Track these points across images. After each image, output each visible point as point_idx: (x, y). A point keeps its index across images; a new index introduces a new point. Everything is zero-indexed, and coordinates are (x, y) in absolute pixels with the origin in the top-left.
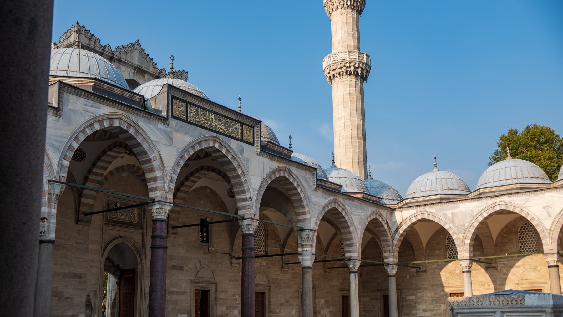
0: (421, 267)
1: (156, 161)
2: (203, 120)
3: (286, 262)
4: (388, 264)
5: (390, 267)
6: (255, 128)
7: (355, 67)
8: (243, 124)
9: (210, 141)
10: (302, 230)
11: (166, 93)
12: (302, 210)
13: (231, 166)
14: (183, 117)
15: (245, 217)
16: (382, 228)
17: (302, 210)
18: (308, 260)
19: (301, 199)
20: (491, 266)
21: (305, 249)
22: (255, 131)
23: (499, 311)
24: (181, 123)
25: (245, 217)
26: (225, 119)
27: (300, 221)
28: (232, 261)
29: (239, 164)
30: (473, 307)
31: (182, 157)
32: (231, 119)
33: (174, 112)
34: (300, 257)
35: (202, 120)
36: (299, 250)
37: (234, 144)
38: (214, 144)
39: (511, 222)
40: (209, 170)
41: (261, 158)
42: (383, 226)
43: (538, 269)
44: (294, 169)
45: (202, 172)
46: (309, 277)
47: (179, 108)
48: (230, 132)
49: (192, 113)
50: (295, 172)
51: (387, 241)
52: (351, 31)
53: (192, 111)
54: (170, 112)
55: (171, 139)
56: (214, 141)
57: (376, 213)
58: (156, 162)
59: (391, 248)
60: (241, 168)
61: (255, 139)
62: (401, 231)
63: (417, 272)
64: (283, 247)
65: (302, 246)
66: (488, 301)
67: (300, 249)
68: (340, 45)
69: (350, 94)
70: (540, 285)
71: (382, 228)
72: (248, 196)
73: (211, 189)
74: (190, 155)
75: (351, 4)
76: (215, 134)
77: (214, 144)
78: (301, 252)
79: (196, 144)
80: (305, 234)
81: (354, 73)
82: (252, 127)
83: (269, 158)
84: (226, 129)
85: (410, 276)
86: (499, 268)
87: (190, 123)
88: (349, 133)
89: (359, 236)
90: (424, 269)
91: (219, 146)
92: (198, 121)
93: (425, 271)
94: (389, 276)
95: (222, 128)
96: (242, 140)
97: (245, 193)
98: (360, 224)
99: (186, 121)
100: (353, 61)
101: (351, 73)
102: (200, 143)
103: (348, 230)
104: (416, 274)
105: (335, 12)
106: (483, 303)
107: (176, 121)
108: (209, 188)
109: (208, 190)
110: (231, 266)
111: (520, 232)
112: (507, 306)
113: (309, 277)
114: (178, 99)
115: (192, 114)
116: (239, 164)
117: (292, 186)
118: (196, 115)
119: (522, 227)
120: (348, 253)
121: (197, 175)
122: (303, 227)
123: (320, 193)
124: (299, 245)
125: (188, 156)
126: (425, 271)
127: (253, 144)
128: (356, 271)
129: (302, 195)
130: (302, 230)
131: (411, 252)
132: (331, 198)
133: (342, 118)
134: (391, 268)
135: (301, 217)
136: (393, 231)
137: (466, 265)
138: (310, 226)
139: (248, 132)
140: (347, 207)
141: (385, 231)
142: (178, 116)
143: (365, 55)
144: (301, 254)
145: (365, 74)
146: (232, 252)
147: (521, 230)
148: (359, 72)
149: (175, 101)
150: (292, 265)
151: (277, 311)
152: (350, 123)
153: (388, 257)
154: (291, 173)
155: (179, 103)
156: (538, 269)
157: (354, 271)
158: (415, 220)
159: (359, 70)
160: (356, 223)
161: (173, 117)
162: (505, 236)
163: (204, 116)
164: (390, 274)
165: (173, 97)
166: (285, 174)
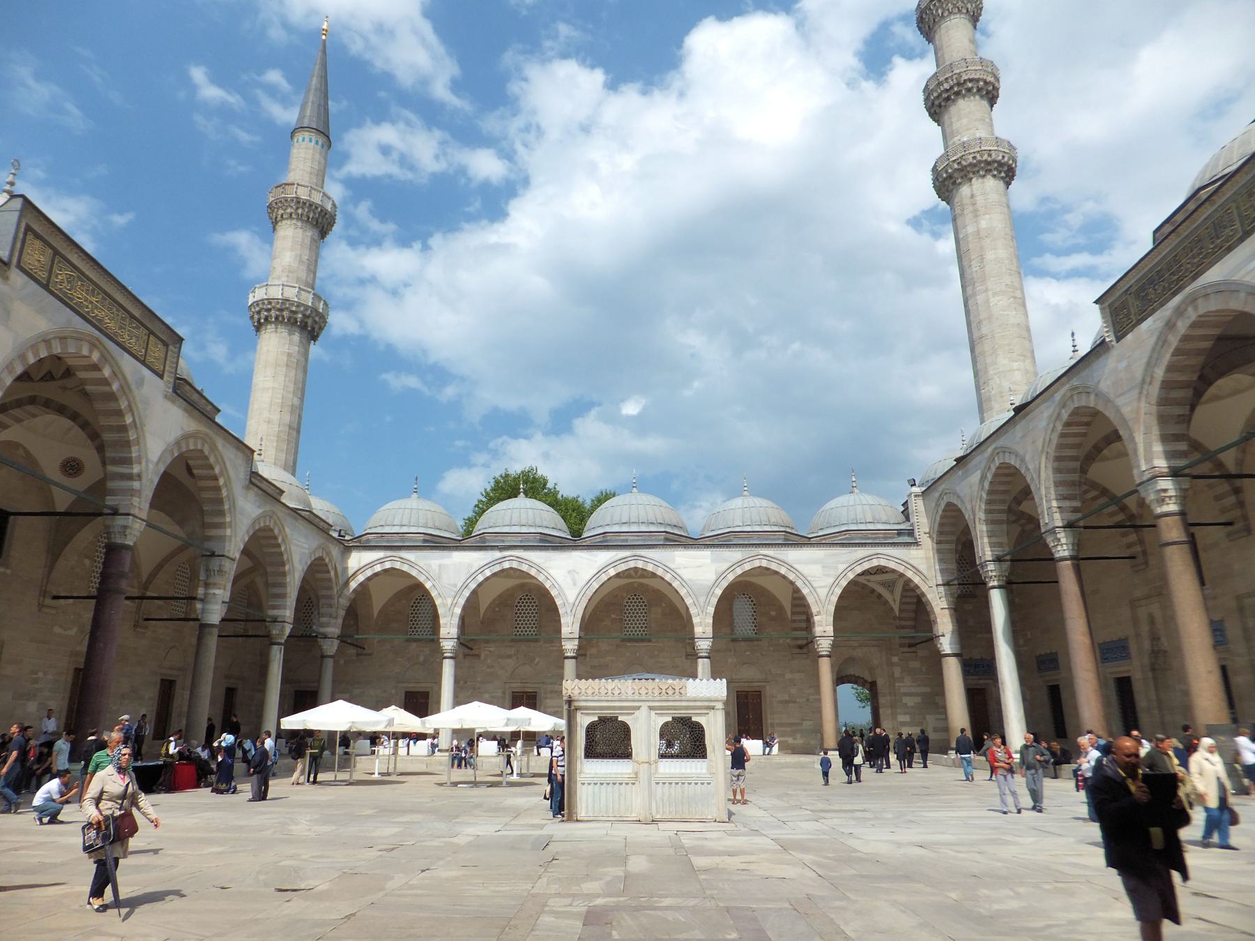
0: (366, 647)
3: (145, 617)
4: (325, 637)
5: (328, 642)
6: (171, 347)
7: (304, 315)
8: (151, 333)
9: (83, 343)
10: (213, 555)
11: (16, 215)
12: (217, 520)
13: (112, 405)
14: (43, 275)
15: (121, 511)
16: (326, 576)
17: (217, 520)
18: (215, 613)
19: (222, 498)
20: (471, 652)
21: (212, 591)
22: (169, 353)
23: (644, 706)
24: (34, 286)
25: (121, 511)
26: (122, 313)
27: (209, 538)
28: (43, 601)
29: (130, 405)
30: (606, 699)
31: (22, 357)
32: (132, 316)
33: (25, 258)
34: (199, 606)
36: (199, 592)
37: (128, 364)
38: (91, 351)
39: (508, 590)
40: (48, 407)
41: (168, 405)
42: (328, 572)
43: (536, 662)
44: (220, 443)
45: (30, 408)
46: (212, 642)
47: (36, 256)
48: (125, 338)
50: (220, 447)
51: (330, 597)
52: (305, 258)
53: (61, 275)
54: (16, 254)
56: (93, 345)
57: (323, 549)
59: (334, 610)
60: (133, 415)
61: (167, 368)
62: (353, 585)
63: (358, 655)
64: (146, 586)
65: (207, 585)
66: (630, 688)
67: (201, 591)
68: (286, 274)
69: (289, 355)
70: (536, 685)
71: (326, 576)
72: (136, 470)
73: (27, 451)
74: (38, 358)
75: (313, 218)
76: (97, 332)
77: (91, 351)
78: (202, 597)
79: (55, 338)
80: (215, 563)
81: (301, 322)
82: (166, 345)
83: (185, 410)
85: (345, 661)
86: (482, 658)
87: (52, 293)
88: (275, 417)
89: (296, 582)
90: (369, 652)
91: (100, 360)
93: (370, 655)
94: (323, 657)
95: (112, 325)
96: (143, 363)
97: (131, 464)
98: (300, 561)
99: (46, 287)
100: (303, 305)
101: (297, 322)
102: (63, 339)
103: (281, 569)
104: (355, 658)
105: (284, 222)
106: (623, 691)
107: (25, 278)
108: (24, 448)
109: (21, 452)
110: (39, 610)
111: (517, 606)
112: (658, 698)
113: (212, 642)
114: (38, 236)
115: (60, 277)
116: (130, 405)
117: (211, 472)
118: (69, 282)
119: (521, 599)
120: (274, 609)
121: (17, 412)
122: (215, 550)
123: (252, 494)
124: (201, 583)
125: (35, 357)
126: (370, 655)
127: (161, 377)
128: (283, 641)
129: (224, 493)
130: (213, 555)
131: (352, 622)
132: (268, 508)
133: (268, 389)
134: (330, 643)
135: (213, 532)
136: (341, 581)
137: (450, 648)
138: (229, 551)
139: (156, 351)
140: (287, 530)
141: (330, 580)
142: (31, 269)
143: (322, 303)
144: (202, 600)
145: (316, 330)
146: (47, 583)
147: (519, 603)
148: (309, 324)
149: (30, 237)
150: (154, 622)
151: (114, 708)
152: (280, 401)
153: (322, 625)
154: (214, 448)
155: (38, 243)
156: (536, 662)
157: (279, 641)
158: (379, 570)
159: (310, 321)
160: (296, 558)
161: (19, 266)
162: (497, 609)
164: (325, 654)
165: (28, 229)
166: (203, 445)
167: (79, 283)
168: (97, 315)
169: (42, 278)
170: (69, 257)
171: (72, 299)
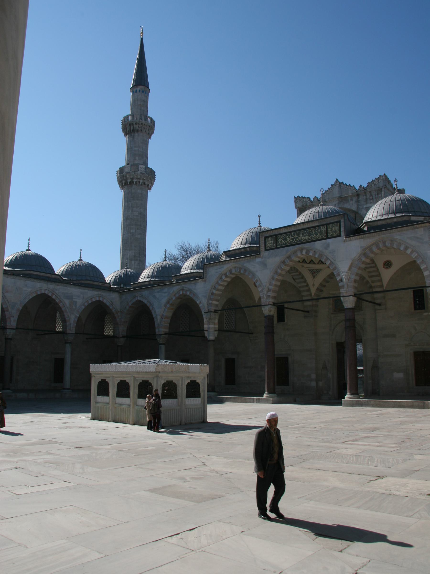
1: (258, 282)
2: (289, 241)
8: (327, 225)
33: (267, 246)
35: (288, 241)
37: (318, 245)
49: (280, 240)
53: (280, 241)
55: (264, 265)
58: (257, 283)
84: (310, 237)
92: (285, 243)
99: (276, 248)
107: (268, 251)
115: (280, 241)
118: (283, 240)
142: (270, 247)
161: (266, 250)
163: (290, 237)
167: (288, 236)
168: (298, 240)
169: (274, 247)
170: (281, 232)
171: (286, 244)
